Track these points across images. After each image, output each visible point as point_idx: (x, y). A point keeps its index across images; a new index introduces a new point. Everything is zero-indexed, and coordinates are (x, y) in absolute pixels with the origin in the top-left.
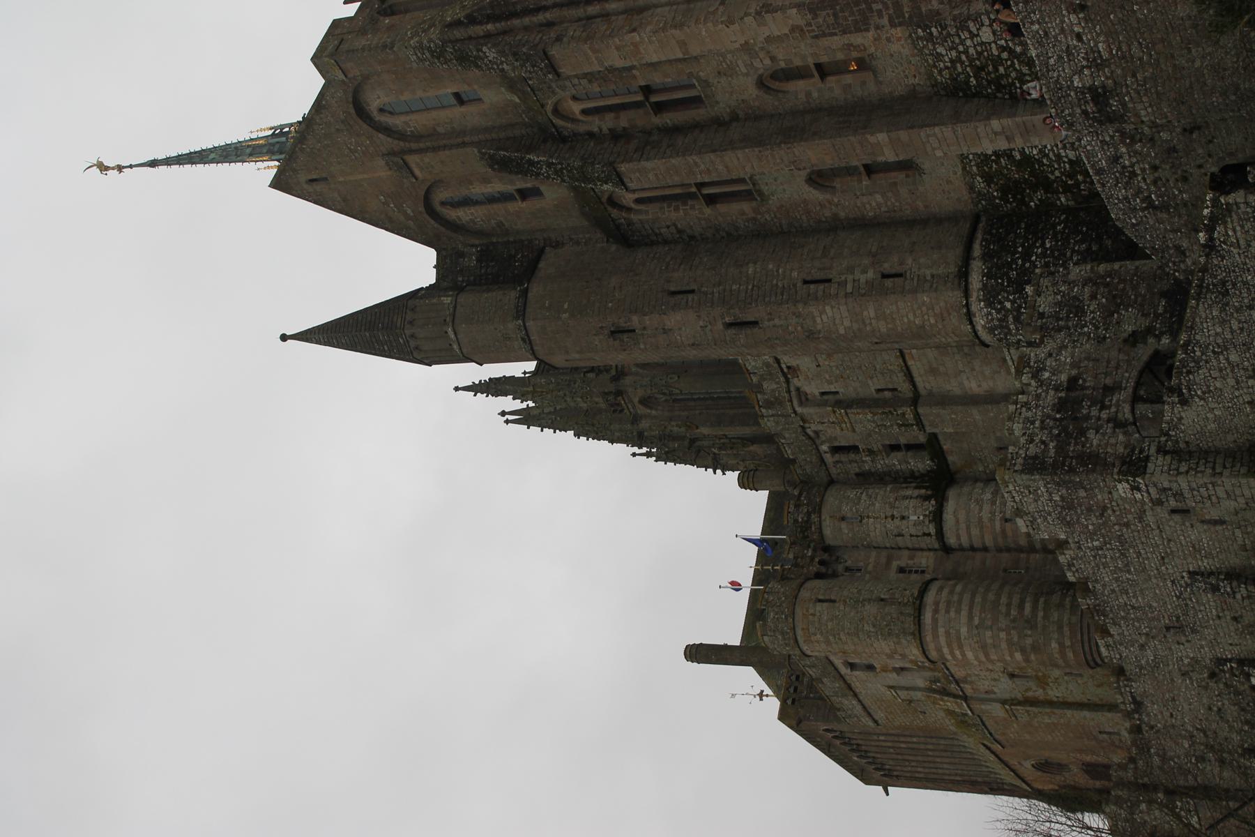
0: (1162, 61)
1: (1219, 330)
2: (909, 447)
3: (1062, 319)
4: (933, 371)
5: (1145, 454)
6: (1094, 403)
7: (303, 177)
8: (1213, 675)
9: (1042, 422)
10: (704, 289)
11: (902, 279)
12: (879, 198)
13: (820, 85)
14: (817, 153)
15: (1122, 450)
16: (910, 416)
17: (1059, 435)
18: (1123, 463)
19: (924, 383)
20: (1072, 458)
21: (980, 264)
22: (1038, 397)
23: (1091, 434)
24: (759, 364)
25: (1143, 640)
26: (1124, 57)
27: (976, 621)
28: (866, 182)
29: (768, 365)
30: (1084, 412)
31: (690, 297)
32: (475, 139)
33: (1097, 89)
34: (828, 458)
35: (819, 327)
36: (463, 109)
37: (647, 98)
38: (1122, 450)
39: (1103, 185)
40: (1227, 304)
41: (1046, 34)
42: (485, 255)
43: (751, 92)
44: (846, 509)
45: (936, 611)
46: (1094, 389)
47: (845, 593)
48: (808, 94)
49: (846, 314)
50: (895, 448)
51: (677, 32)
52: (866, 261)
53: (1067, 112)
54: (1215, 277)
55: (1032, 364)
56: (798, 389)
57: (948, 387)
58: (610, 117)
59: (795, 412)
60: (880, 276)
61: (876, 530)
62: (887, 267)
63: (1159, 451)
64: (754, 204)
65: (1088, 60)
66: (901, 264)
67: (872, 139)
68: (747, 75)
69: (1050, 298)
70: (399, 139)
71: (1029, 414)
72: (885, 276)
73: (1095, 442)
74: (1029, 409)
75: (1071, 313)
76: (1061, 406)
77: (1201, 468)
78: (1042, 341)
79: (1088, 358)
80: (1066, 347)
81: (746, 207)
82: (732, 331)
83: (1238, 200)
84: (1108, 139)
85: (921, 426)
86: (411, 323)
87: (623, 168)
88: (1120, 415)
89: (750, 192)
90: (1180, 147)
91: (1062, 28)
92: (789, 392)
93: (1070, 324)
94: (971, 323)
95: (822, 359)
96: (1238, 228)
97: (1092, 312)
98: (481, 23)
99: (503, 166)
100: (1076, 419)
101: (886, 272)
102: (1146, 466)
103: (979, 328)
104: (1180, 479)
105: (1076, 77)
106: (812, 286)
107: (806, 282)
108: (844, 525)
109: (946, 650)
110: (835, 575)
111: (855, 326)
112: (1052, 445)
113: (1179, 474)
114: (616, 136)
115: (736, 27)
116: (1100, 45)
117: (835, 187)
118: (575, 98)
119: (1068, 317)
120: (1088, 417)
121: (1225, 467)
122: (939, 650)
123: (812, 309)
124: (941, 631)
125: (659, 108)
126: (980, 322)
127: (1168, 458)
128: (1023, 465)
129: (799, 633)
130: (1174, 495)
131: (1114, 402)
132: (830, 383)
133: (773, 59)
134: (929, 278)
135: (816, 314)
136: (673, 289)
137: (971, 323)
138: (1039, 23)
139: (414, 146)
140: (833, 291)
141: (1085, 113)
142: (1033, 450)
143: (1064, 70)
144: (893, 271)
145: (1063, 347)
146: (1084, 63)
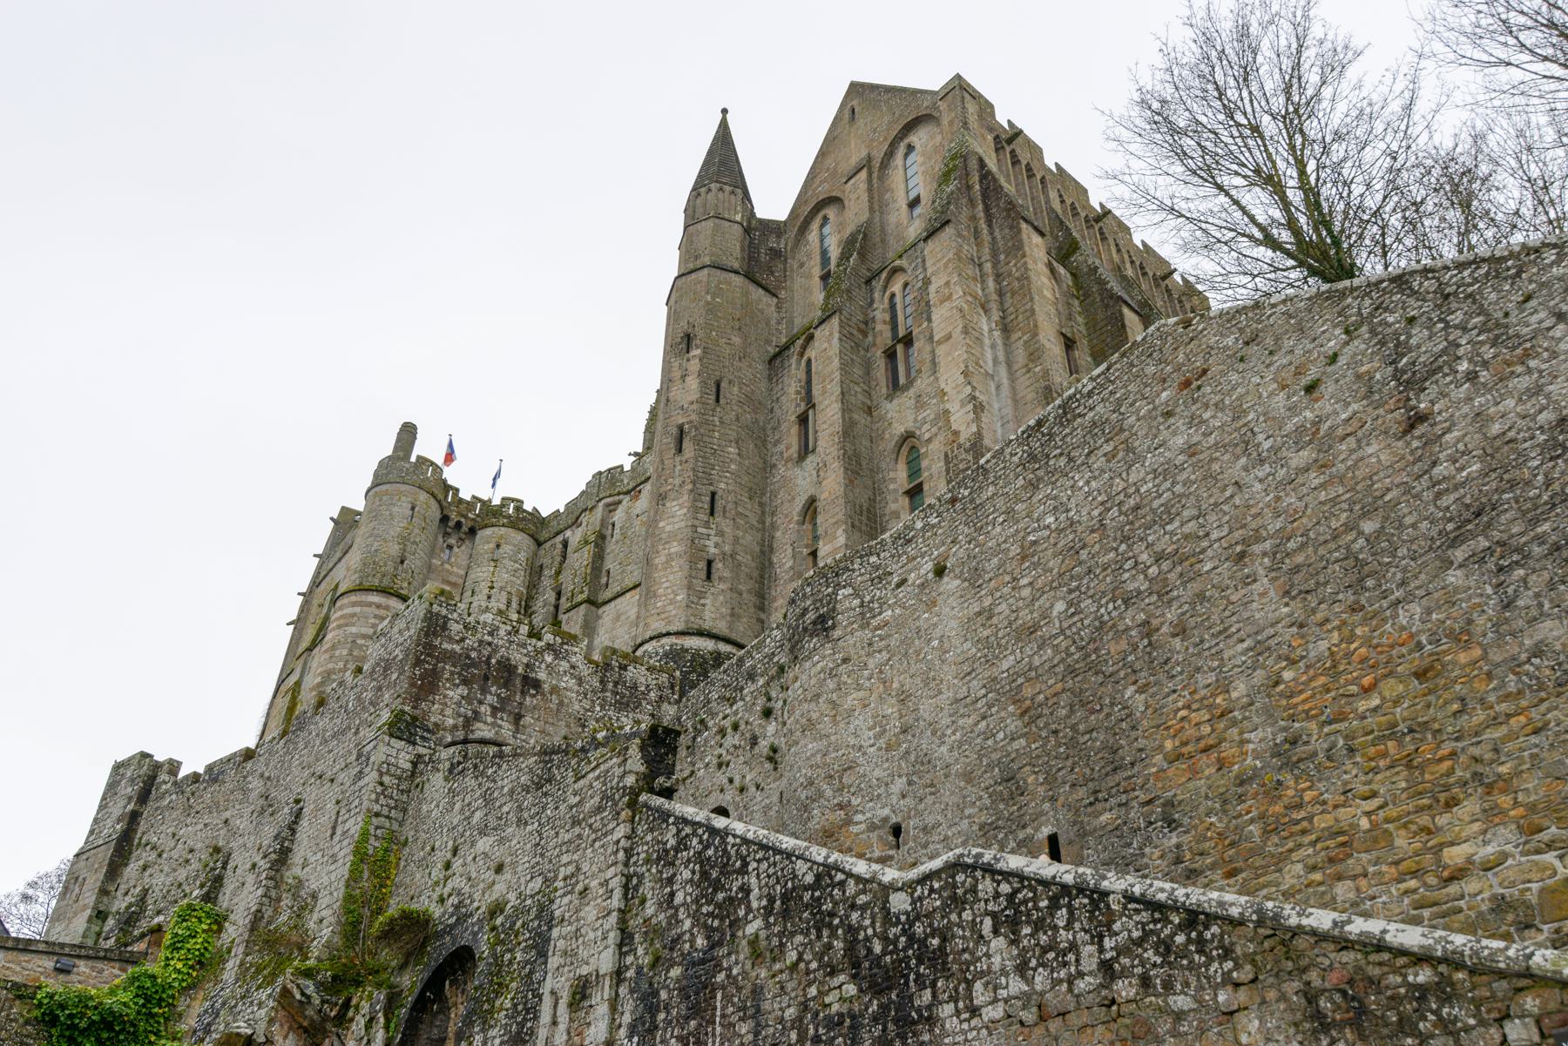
0: (861, 694)
1: (506, 790)
2: (557, 607)
3: (615, 686)
4: (618, 618)
5: (418, 741)
6: (502, 700)
7: (855, 103)
8: (217, 850)
9: (490, 644)
10: (718, 409)
11: (704, 577)
12: (790, 563)
13: (901, 492)
14: (832, 485)
15: (432, 719)
16: (580, 598)
17: (468, 657)
18: (415, 719)
19: (608, 612)
20: (436, 665)
21: (710, 648)
22: (524, 645)
23: (463, 690)
24: (647, 466)
25: (267, 774)
26: (870, 645)
27: (359, 642)
28: (805, 551)
29: (646, 471)
30: (493, 689)
31: (713, 397)
32: (877, 219)
33: (833, 618)
34: (560, 538)
35: (668, 504)
36: (905, 207)
37: (899, 341)
38: (432, 719)
39: (725, 672)
40: (528, 792)
41: (909, 541)
42: (776, 254)
43: (899, 429)
44: (506, 548)
45: (379, 606)
46: (520, 704)
47: (416, 531)
48: (893, 480)
49: (676, 526)
50: (559, 594)
51: (960, 329)
52: (727, 548)
53: (808, 589)
54: (558, 768)
55: (565, 647)
56: (620, 502)
57: (601, 632)
58: (887, 317)
59: (600, 500)
60: (711, 557)
61: (482, 573)
62: (718, 565)
63: (419, 756)
64: (796, 455)
65: (872, 601)
66: (720, 578)
67: (840, 532)
68: (916, 420)
69: (643, 680)
70: (882, 163)
71: (502, 633)
72: (710, 563)
73: (451, 693)
74: (510, 634)
75: (622, 698)
76: (507, 668)
77: (382, 801)
78: (591, 662)
79: (561, 704)
80: (580, 685)
81: (794, 451)
82: (675, 431)
83: (629, 761)
84: (776, 659)
85: (568, 611)
86: (721, 189)
87: (835, 321)
88: (479, 725)
89: (805, 450)
90: (756, 750)
91: (914, 559)
92: (619, 494)
93: (608, 694)
94: (651, 639)
95: (644, 518)
96: (597, 772)
97: (618, 719)
98: (981, 181)
99: (849, 246)
100: (486, 678)
101: (714, 565)
102: (401, 739)
103: (646, 647)
104: (375, 775)
105: (850, 591)
106: (708, 499)
107: (713, 494)
108: (492, 545)
109: (339, 614)
110: (446, 535)
111: (664, 536)
112: (457, 648)
113: (381, 774)
114: (867, 324)
115: (961, 379)
116: (890, 612)
117: (803, 523)
118: (906, 285)
119: (617, 693)
120: (484, 691)
121: (377, 828)
122: (341, 608)
123: (686, 497)
124: (357, 609)
125: (891, 355)
126: (648, 647)
127: (408, 766)
128: (438, 614)
129: (384, 488)
130: (360, 772)
131: (499, 722)
132: (621, 529)
133: (929, 440)
134: (702, 601)
135: (681, 501)
136: (722, 385)
137: (651, 639)
138: (924, 527)
139: (875, 175)
140: (701, 516)
141: (805, 611)
142: (455, 628)
143: (861, 575)
144: (713, 571)
145: (580, 681)
146: (867, 598)
